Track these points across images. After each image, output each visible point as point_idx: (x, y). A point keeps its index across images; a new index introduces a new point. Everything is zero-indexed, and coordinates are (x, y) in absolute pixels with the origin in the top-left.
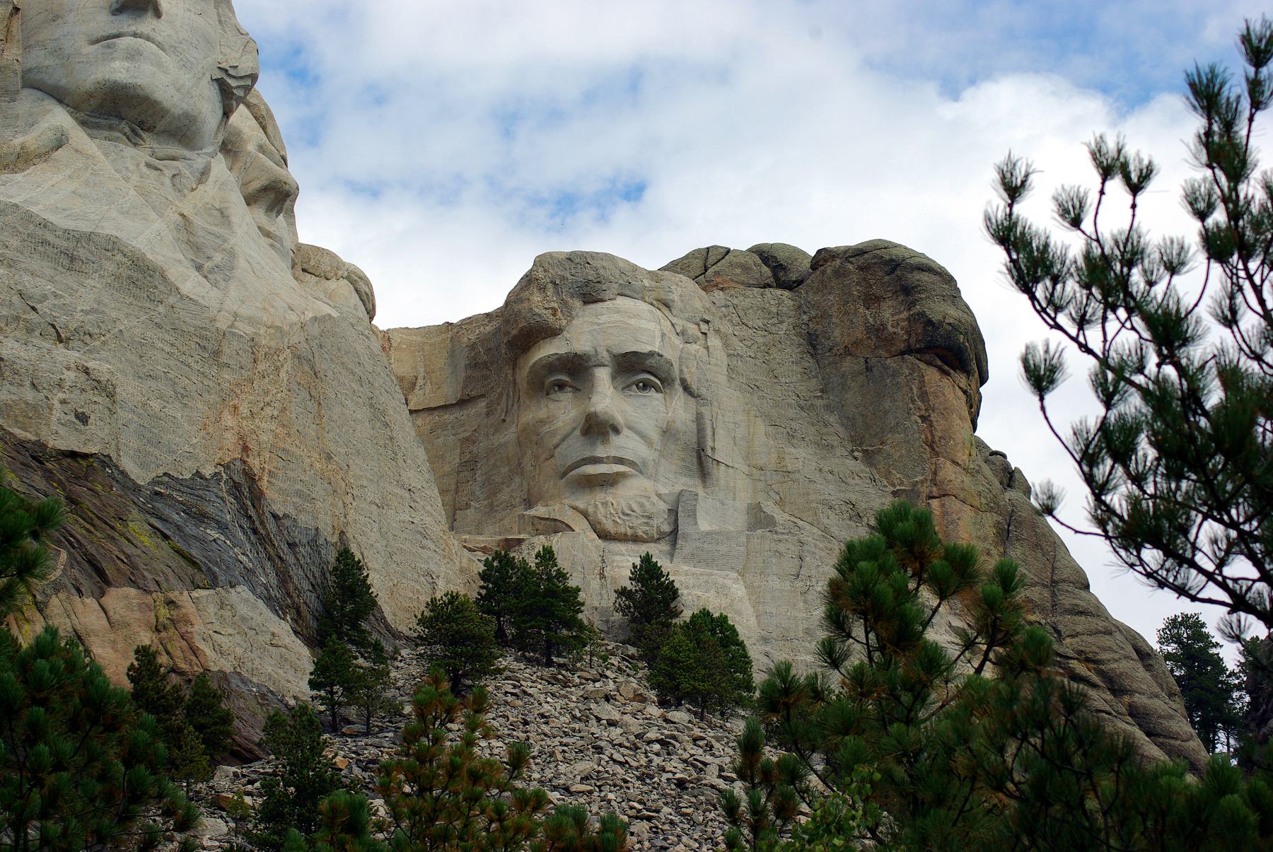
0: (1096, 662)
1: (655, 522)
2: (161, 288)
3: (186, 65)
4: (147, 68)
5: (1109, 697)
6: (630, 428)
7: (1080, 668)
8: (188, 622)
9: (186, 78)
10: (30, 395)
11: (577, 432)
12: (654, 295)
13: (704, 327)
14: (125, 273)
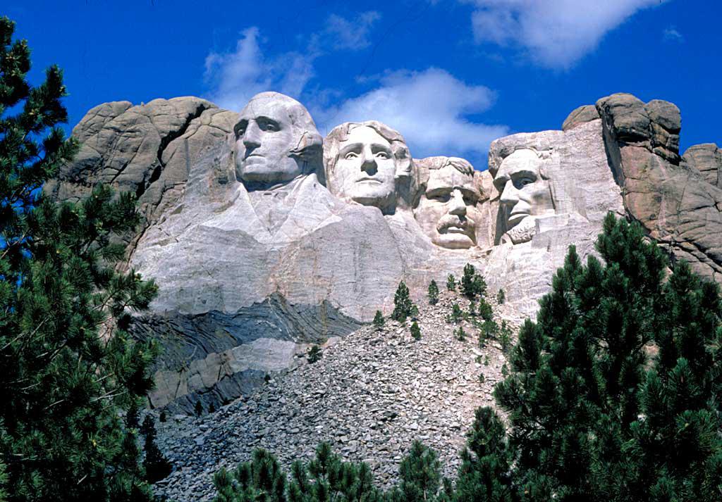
0: (693, 240)
1: (529, 233)
2: (252, 242)
3: (271, 159)
4: (255, 165)
5: (698, 253)
6: (521, 199)
7: (685, 245)
8: (229, 359)
9: (274, 162)
10: (189, 299)
12: (530, 145)
13: (551, 151)
14: (241, 240)
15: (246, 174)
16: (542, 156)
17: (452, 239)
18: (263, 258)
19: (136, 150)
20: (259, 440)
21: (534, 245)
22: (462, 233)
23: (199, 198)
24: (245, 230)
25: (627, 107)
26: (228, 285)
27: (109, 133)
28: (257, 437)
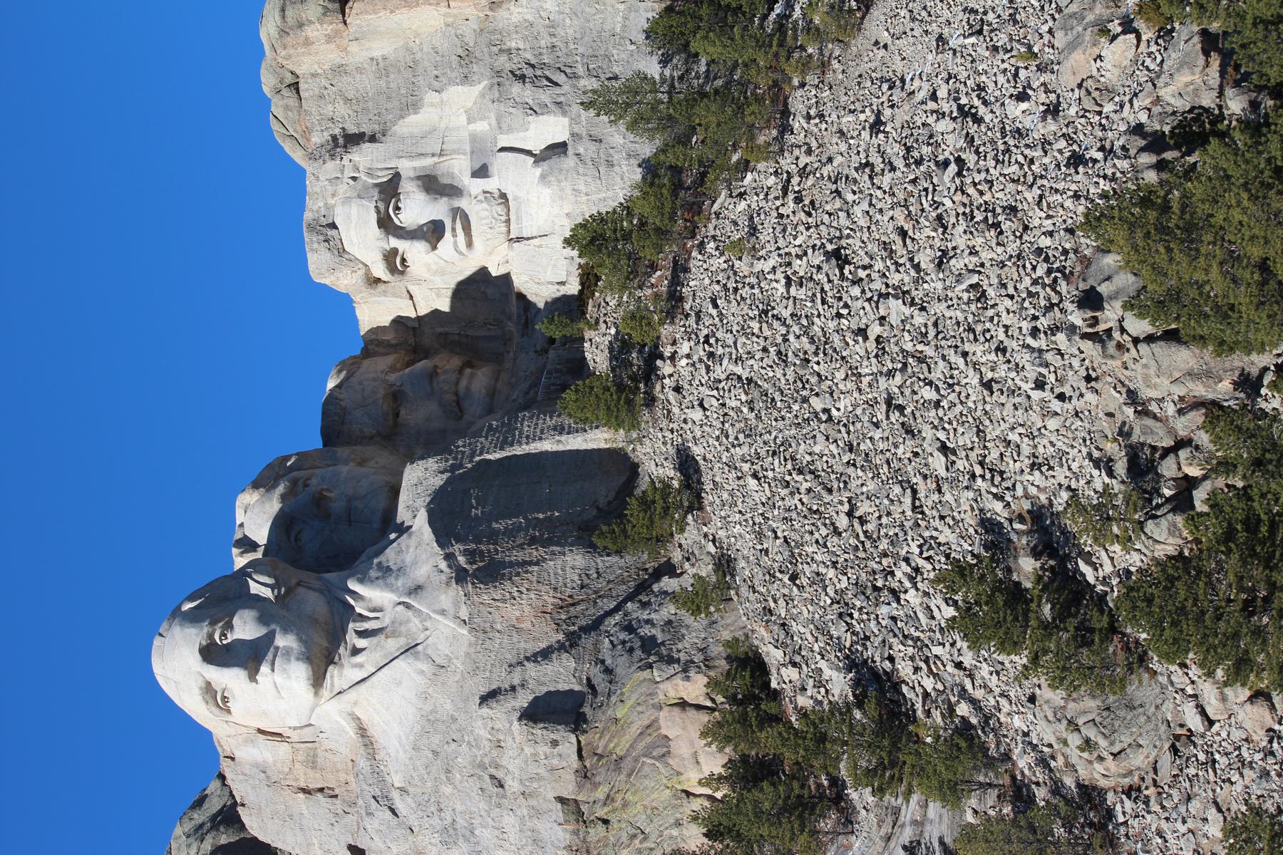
13: (345, 161)
16: (354, 179)
17: (484, 391)
18: (480, 635)
22: (472, 376)
23: (340, 811)
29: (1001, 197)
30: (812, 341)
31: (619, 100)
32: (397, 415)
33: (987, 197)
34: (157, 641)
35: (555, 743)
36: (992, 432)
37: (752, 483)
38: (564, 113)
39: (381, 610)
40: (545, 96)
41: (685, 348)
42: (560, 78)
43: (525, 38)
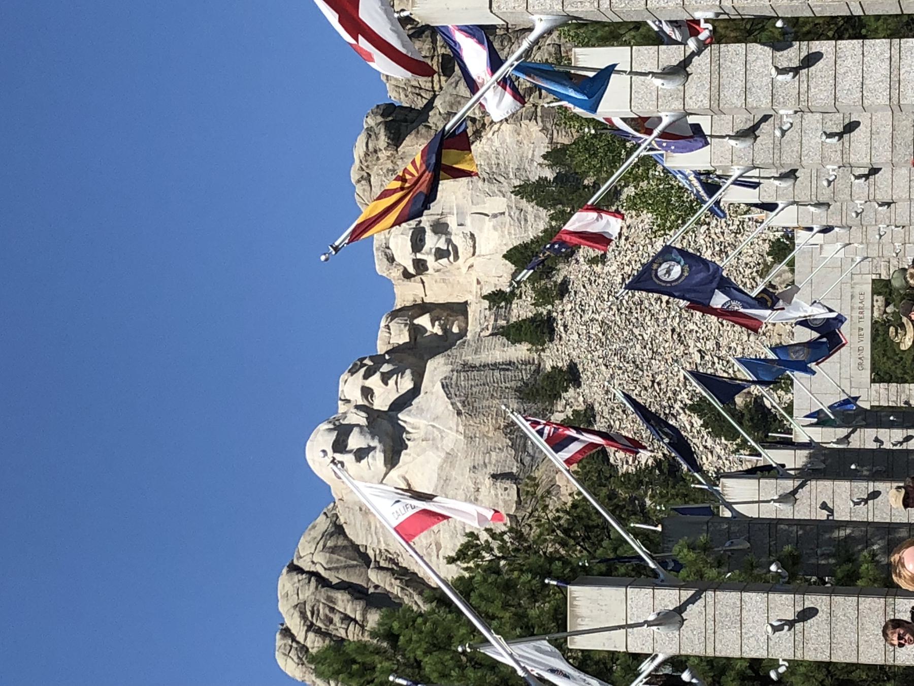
10: (501, 503)
11: (440, 261)
15: (386, 464)
19: (332, 610)
20: (656, 385)
21: (481, 230)
24: (440, 460)
25: (370, 136)
26: (491, 470)
27: (311, 635)
28: (653, 385)
29: (729, 238)
30: (634, 304)
31: (531, 191)
32: (415, 339)
33: (722, 239)
34: (308, 443)
35: (506, 489)
36: (723, 342)
37: (603, 368)
38: (504, 196)
39: (419, 428)
40: (495, 188)
41: (569, 306)
42: (501, 179)
43: (485, 160)
